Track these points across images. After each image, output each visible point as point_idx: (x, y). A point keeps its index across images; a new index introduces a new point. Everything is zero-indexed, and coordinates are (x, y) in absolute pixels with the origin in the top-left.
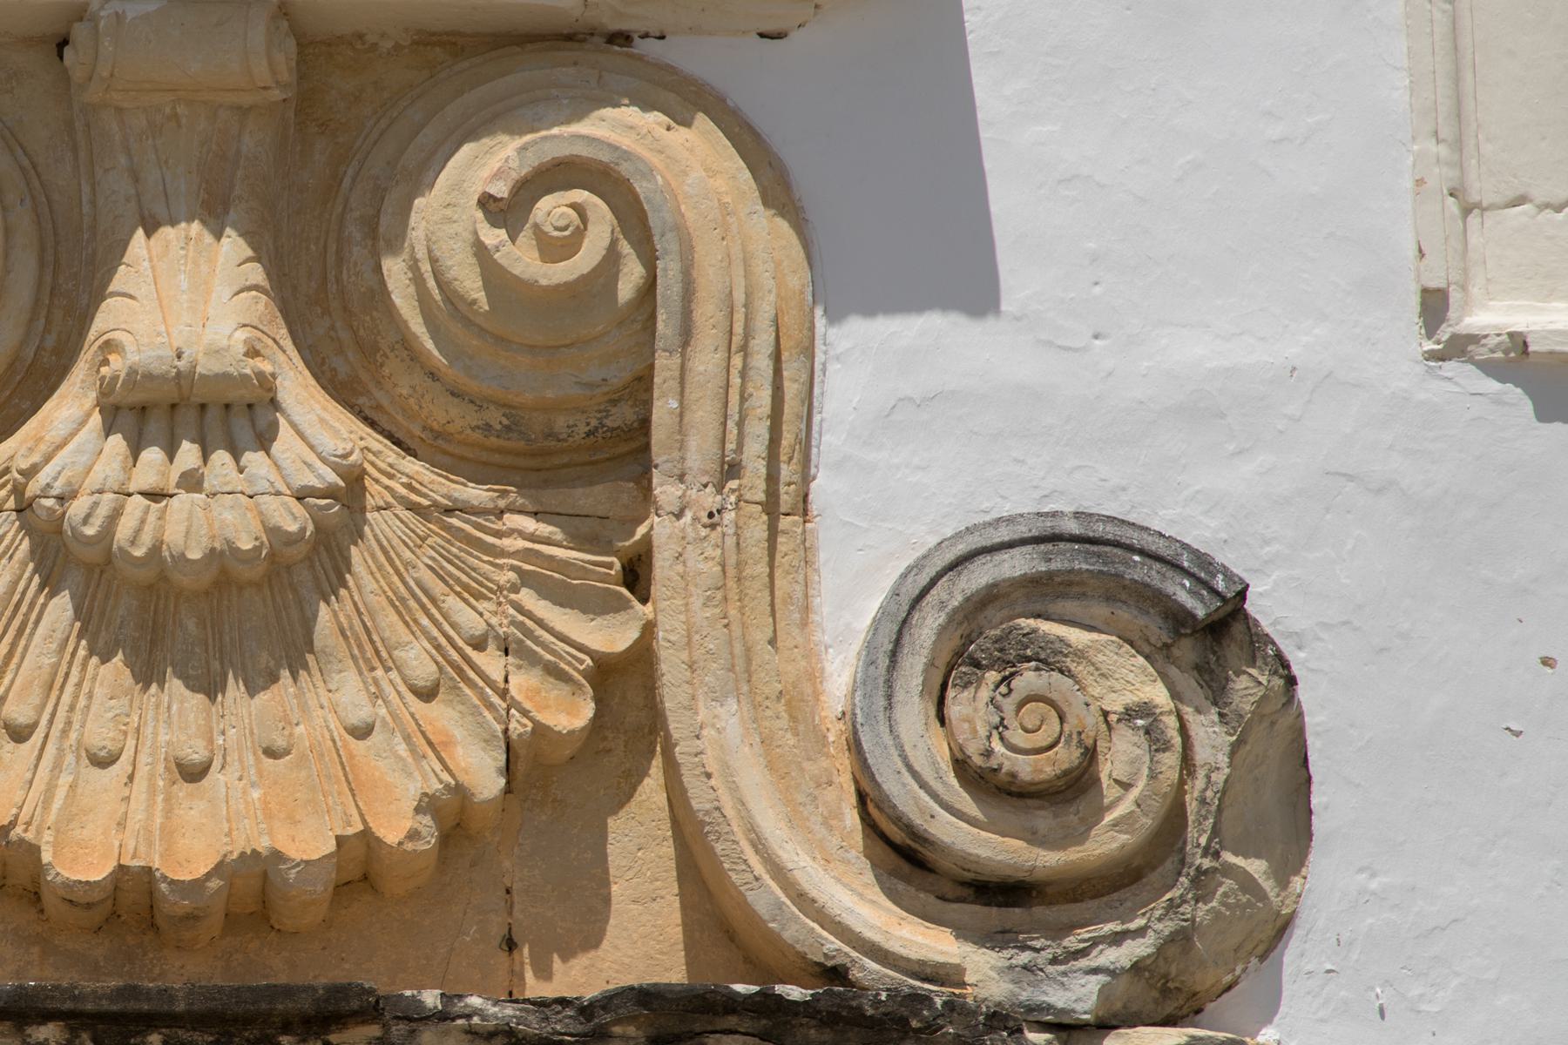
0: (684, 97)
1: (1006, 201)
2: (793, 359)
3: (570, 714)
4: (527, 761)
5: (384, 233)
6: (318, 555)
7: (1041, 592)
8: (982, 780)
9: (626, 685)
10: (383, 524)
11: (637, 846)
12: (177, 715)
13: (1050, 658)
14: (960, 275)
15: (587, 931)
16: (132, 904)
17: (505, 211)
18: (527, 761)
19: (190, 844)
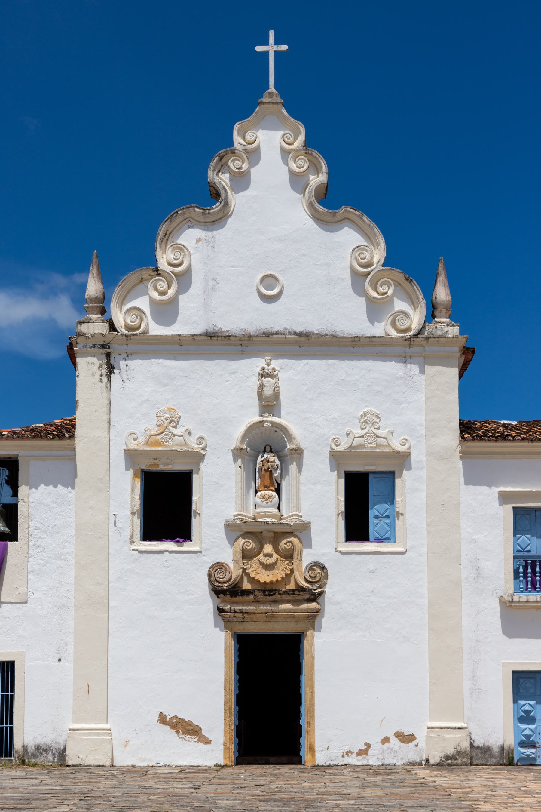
0: (296, 536)
1: (313, 542)
2: (301, 551)
3: (289, 572)
4: (287, 575)
5: (279, 545)
6: (275, 564)
7: (314, 566)
8: (310, 576)
9: (292, 570)
10: (279, 561)
11: (292, 579)
12: (267, 572)
13: (315, 570)
14: (310, 546)
15: (289, 583)
16: (265, 583)
17: (286, 544)
18: (287, 575)
19: (268, 580)
